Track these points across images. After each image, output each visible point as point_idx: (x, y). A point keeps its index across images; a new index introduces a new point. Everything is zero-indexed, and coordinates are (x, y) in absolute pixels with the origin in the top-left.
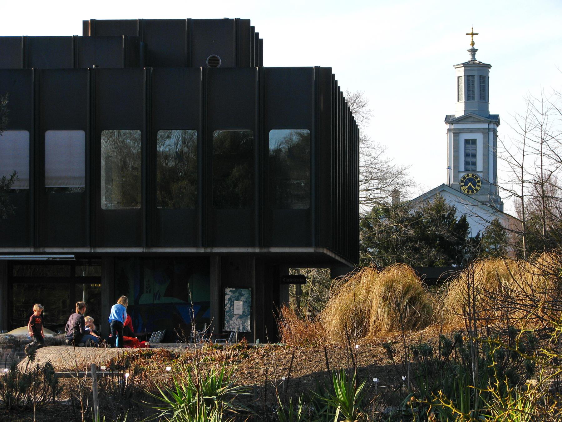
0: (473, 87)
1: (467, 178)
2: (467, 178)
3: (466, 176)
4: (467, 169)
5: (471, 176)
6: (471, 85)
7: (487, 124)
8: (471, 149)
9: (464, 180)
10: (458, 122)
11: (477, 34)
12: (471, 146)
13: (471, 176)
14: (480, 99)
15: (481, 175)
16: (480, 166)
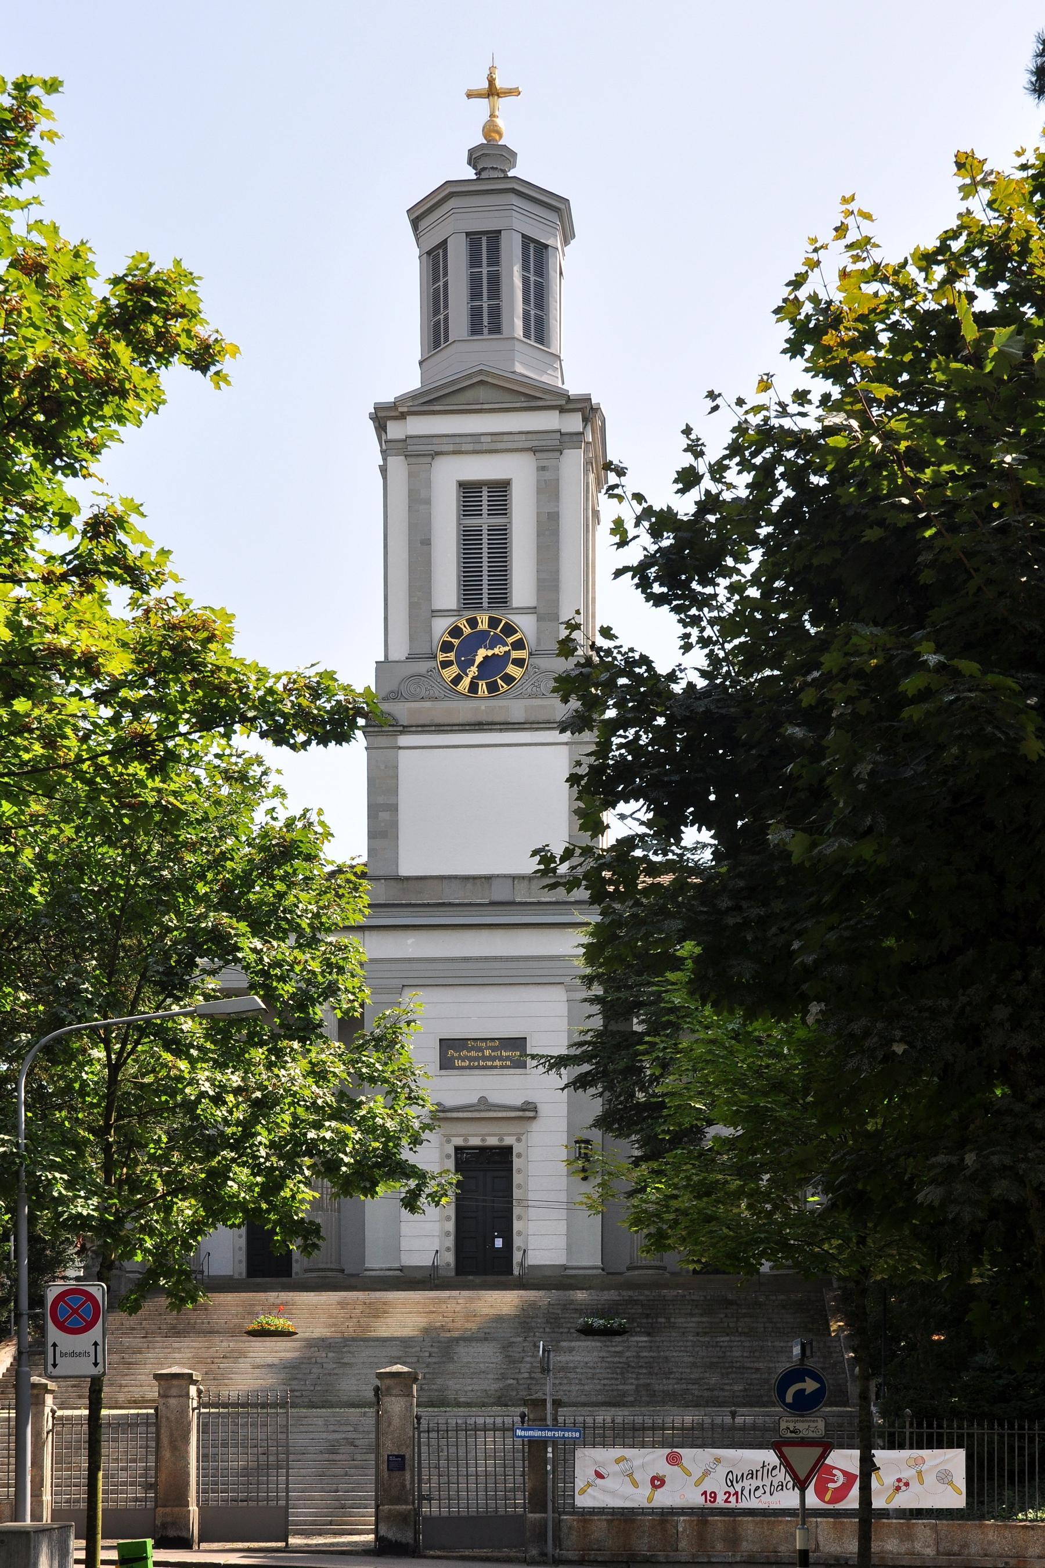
2: (467, 630)
3: (463, 624)
5: (483, 625)
8: (485, 522)
9: (456, 642)
12: (485, 512)
13: (483, 625)
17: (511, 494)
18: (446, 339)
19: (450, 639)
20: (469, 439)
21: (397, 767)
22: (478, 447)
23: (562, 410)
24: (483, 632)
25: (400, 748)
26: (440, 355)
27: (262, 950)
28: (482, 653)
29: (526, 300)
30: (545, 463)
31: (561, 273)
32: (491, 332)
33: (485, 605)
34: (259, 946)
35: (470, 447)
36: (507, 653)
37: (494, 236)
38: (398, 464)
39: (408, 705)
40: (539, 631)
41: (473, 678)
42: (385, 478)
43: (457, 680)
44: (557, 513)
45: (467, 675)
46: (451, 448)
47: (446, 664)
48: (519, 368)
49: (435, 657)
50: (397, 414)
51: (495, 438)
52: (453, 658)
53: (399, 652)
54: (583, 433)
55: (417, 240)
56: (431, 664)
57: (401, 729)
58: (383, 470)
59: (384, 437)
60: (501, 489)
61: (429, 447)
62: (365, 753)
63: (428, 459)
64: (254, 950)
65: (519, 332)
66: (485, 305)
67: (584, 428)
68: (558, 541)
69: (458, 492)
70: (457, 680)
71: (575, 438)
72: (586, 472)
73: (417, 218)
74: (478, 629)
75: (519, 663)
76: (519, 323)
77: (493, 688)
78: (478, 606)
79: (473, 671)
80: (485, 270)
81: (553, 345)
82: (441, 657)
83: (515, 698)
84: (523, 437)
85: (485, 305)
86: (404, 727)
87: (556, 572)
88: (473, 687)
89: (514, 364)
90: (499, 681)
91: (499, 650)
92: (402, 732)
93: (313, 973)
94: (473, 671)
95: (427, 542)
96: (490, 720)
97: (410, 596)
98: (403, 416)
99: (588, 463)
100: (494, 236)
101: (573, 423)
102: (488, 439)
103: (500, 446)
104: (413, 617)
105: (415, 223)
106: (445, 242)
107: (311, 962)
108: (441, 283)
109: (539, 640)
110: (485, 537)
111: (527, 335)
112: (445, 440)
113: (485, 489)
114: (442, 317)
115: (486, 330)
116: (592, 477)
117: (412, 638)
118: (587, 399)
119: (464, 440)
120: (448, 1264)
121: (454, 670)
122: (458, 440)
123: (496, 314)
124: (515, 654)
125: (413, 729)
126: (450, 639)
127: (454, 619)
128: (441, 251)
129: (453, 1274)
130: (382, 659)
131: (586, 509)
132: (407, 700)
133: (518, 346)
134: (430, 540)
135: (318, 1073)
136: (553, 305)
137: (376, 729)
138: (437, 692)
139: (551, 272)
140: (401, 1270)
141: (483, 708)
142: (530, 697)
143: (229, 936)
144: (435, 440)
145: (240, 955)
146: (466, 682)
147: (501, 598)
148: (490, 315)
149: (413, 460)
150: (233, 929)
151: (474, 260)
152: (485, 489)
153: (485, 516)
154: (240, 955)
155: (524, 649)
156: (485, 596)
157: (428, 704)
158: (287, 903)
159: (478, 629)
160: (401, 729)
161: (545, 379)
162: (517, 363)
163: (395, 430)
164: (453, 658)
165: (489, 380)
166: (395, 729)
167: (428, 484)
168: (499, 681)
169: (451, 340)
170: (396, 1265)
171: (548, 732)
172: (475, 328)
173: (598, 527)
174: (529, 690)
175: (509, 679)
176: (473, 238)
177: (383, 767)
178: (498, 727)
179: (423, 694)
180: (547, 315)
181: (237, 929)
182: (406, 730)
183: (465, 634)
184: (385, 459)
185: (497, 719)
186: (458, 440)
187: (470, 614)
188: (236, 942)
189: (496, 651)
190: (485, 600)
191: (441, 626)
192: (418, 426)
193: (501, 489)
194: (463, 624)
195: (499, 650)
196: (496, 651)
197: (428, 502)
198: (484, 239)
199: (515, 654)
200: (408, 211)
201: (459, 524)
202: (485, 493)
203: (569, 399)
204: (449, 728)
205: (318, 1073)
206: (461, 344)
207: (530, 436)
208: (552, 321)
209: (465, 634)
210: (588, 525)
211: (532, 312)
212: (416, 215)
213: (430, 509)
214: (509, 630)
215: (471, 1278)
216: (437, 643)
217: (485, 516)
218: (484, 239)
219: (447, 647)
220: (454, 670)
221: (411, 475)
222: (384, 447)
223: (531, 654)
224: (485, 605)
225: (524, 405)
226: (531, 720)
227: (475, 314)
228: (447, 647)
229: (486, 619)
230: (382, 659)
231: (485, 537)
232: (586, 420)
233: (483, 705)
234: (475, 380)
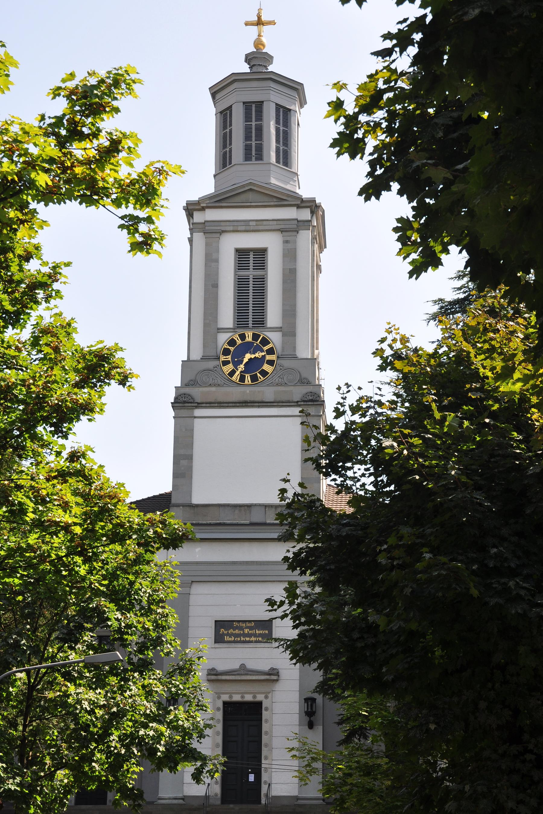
1: (239, 342)
2: (239, 342)
3: (236, 337)
5: (249, 339)
8: (251, 273)
9: (232, 349)
12: (251, 267)
13: (249, 339)
15: (275, 338)
17: (267, 257)
18: (230, 163)
19: (228, 347)
20: (243, 223)
21: (193, 430)
22: (248, 228)
23: (298, 207)
24: (249, 343)
25: (195, 417)
26: (226, 172)
27: (121, 619)
28: (248, 356)
29: (278, 141)
30: (288, 238)
31: (298, 124)
32: (257, 159)
33: (250, 325)
34: (120, 617)
35: (243, 228)
36: (264, 357)
37: (260, 105)
38: (199, 237)
39: (201, 389)
40: (284, 343)
41: (241, 372)
42: (191, 245)
43: (232, 373)
44: (295, 269)
45: (237, 370)
46: (231, 228)
47: (225, 363)
48: (273, 181)
49: (219, 358)
50: (200, 208)
51: (258, 223)
52: (230, 359)
53: (197, 355)
54: (311, 221)
55: (215, 105)
56: (216, 363)
57: (196, 405)
58: (191, 240)
59: (191, 221)
60: (261, 253)
61: (219, 228)
62: (173, 420)
63: (218, 235)
64: (117, 619)
65: (273, 160)
66: (254, 144)
67: (312, 217)
68: (295, 287)
69: (235, 255)
70: (232, 373)
71: (306, 224)
72: (313, 243)
73: (215, 92)
74: (246, 341)
75: (271, 363)
76: (273, 155)
77: (254, 378)
78: (246, 327)
79: (241, 367)
80: (254, 123)
81: (293, 168)
82: (223, 358)
83: (268, 385)
84: (275, 223)
85: (254, 144)
86: (198, 403)
87: (294, 305)
88: (242, 379)
89: (270, 179)
90: (258, 374)
91: (259, 355)
92: (197, 407)
93: (148, 630)
94: (241, 367)
95: (216, 286)
96: (252, 399)
97: (204, 319)
98: (203, 209)
99: (314, 238)
100: (260, 105)
101: (305, 214)
102: (254, 223)
103: (261, 228)
104: (206, 333)
105: (214, 95)
106: (231, 107)
107: (147, 623)
108: (228, 130)
109: (283, 348)
110: (251, 283)
111: (278, 161)
112: (228, 224)
113: (251, 254)
114: (228, 150)
115: (254, 158)
116: (316, 246)
117: (205, 346)
118: (313, 201)
119: (239, 224)
120: (216, 795)
121: (230, 367)
122: (236, 224)
123: (260, 149)
124: (268, 357)
125: (204, 405)
126: (228, 347)
127: (231, 334)
128: (228, 112)
129: (219, 802)
130: (186, 359)
131: (313, 267)
132: (200, 386)
133: (272, 168)
134: (217, 284)
135: (149, 693)
136: (294, 144)
137: (181, 405)
138: (219, 381)
139: (293, 125)
140: (183, 799)
141: (248, 392)
142: (277, 385)
143: (104, 612)
144: (222, 224)
145: (109, 623)
146: (236, 377)
147: (260, 322)
148: (256, 149)
149: (208, 235)
150: (107, 608)
151: (248, 117)
152: (251, 254)
153: (251, 270)
154: (109, 623)
155: (274, 354)
156: (251, 319)
157: (213, 389)
158: (135, 587)
159: (246, 341)
160: (196, 405)
161: (288, 187)
162: (272, 178)
163: (198, 217)
164: (230, 359)
165: (255, 188)
166: (193, 405)
167: (217, 251)
168: (258, 374)
169: (233, 163)
170: (180, 795)
171: (288, 409)
172: (248, 157)
173: (320, 275)
174: (277, 380)
175: (264, 373)
176: (247, 105)
177: (184, 430)
178: (257, 404)
179: (211, 382)
180: (290, 149)
181: (109, 608)
182: (199, 405)
183: (238, 344)
184: (191, 234)
185: (257, 399)
186: (236, 224)
187: (241, 331)
188: (108, 615)
190: (250, 322)
191: (223, 339)
192: (212, 215)
193: (261, 253)
194: (236, 337)
195: (259, 355)
197: (217, 261)
198: (254, 106)
199: (268, 357)
200: (209, 88)
201: (235, 275)
202: (251, 256)
203: (302, 201)
204: (226, 405)
205: (149, 693)
206: (239, 166)
207: (279, 222)
208: (293, 153)
209: (238, 344)
210: (313, 277)
211: (281, 148)
212: (213, 91)
213: (218, 265)
214: (265, 342)
215: (232, 806)
216: (220, 350)
217: (251, 270)
218: (254, 106)
219: (226, 352)
220: (230, 367)
221: (207, 245)
222: (191, 226)
223: (278, 357)
224: (250, 325)
225: (276, 203)
226: (278, 400)
227: (248, 149)
228: (226, 352)
229: (251, 334)
230: (186, 359)
231: (251, 283)
232: (312, 213)
233: (248, 390)
234: (247, 188)
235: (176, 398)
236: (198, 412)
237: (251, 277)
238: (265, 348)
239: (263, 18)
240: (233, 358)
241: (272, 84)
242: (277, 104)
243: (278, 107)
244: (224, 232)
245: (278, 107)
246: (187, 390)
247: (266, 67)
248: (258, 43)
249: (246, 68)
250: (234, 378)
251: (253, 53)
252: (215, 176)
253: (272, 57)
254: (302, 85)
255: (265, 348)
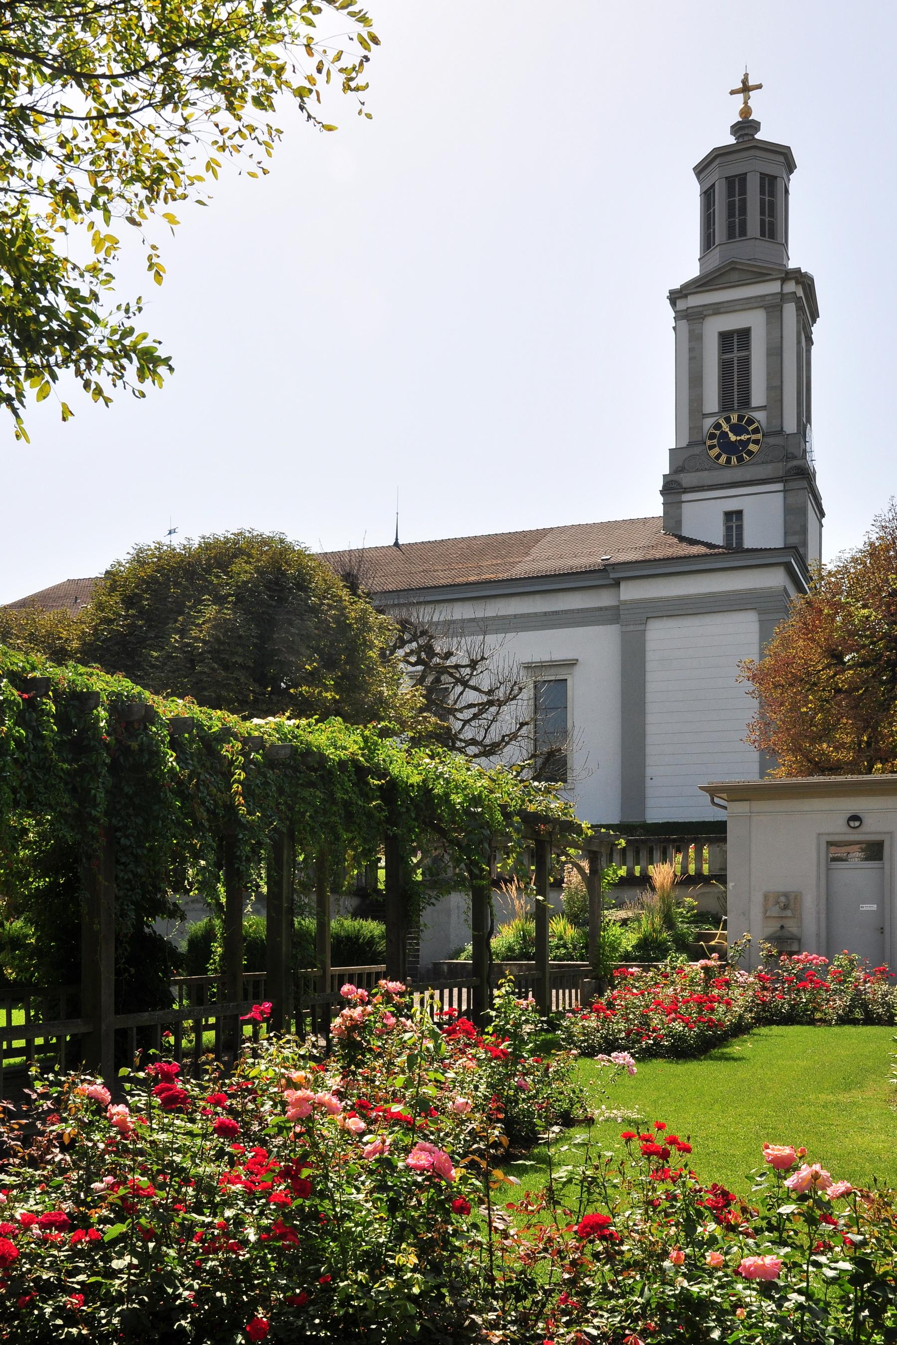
0: (743, 202)
4: (726, 405)
6: (737, 199)
7: (779, 283)
8: (735, 355)
10: (700, 289)
11: (759, 87)
14: (763, 234)
15: (760, 416)
16: (758, 396)
28: (733, 438)
32: (740, 236)
37: (743, 178)
47: (711, 447)
49: (705, 443)
75: (756, 442)
77: (740, 459)
78: (732, 410)
82: (709, 443)
92: (684, 492)
101: (791, 287)
124: (754, 437)
147: (745, 402)
151: (730, 193)
163: (682, 305)
172: (731, 235)
175: (750, 453)
176: (730, 181)
182: (686, 490)
187: (725, 415)
189: (742, 437)
190: (736, 404)
191: (709, 423)
196: (742, 437)
199: (754, 437)
201: (719, 359)
202: (735, 337)
214: (751, 421)
219: (712, 436)
223: (763, 436)
224: (736, 407)
229: (736, 416)
235: (664, 486)
236: (685, 497)
237: (735, 358)
238: (750, 428)
239: (751, 83)
240: (718, 441)
241: (758, 153)
242: (761, 174)
243: (763, 176)
244: (705, 316)
245: (763, 176)
246: (675, 477)
247: (753, 135)
248: (746, 111)
249: (732, 140)
250: (720, 461)
251: (739, 122)
252: (699, 260)
253: (759, 123)
254: (789, 148)
255: (750, 428)
